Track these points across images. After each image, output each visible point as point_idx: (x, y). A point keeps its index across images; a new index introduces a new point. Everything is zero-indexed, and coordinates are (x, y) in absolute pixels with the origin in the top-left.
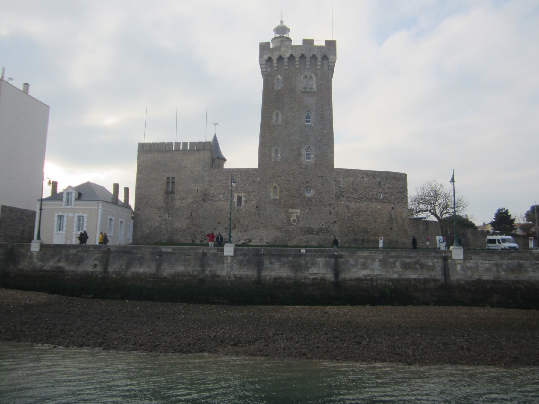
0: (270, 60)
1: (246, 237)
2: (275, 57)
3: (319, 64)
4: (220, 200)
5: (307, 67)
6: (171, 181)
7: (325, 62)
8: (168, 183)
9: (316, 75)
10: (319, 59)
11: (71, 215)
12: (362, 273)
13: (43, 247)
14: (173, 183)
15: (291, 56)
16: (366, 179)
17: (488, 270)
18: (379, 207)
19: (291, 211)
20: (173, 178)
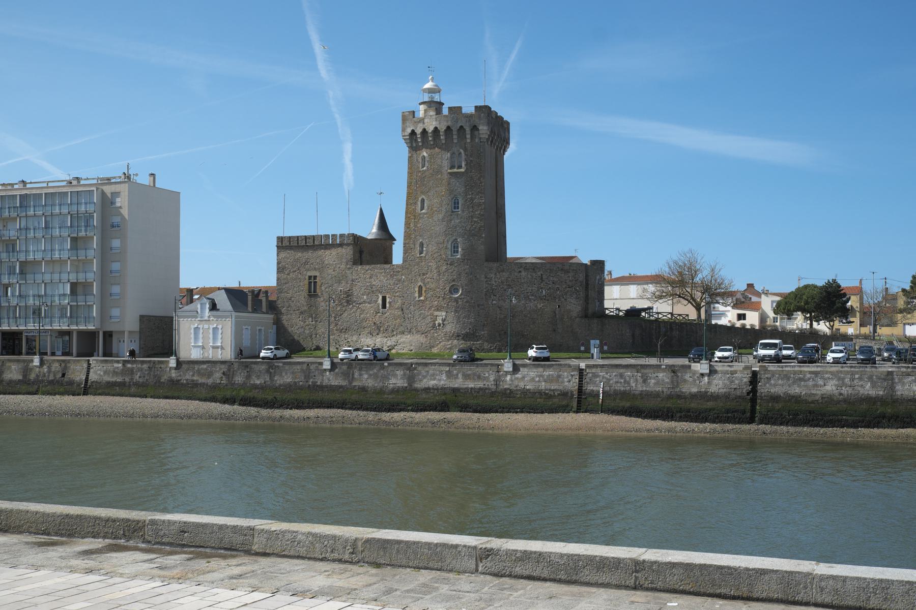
0: (413, 133)
1: (389, 343)
2: (419, 131)
3: (468, 136)
4: (364, 302)
5: (455, 141)
6: (312, 282)
7: (476, 133)
8: (310, 283)
9: (465, 150)
10: (468, 130)
11: (206, 326)
12: (432, 383)
13: (179, 363)
14: (315, 283)
15: (436, 128)
16: (523, 274)
17: (533, 380)
18: (539, 306)
19: (436, 313)
20: (315, 277)
